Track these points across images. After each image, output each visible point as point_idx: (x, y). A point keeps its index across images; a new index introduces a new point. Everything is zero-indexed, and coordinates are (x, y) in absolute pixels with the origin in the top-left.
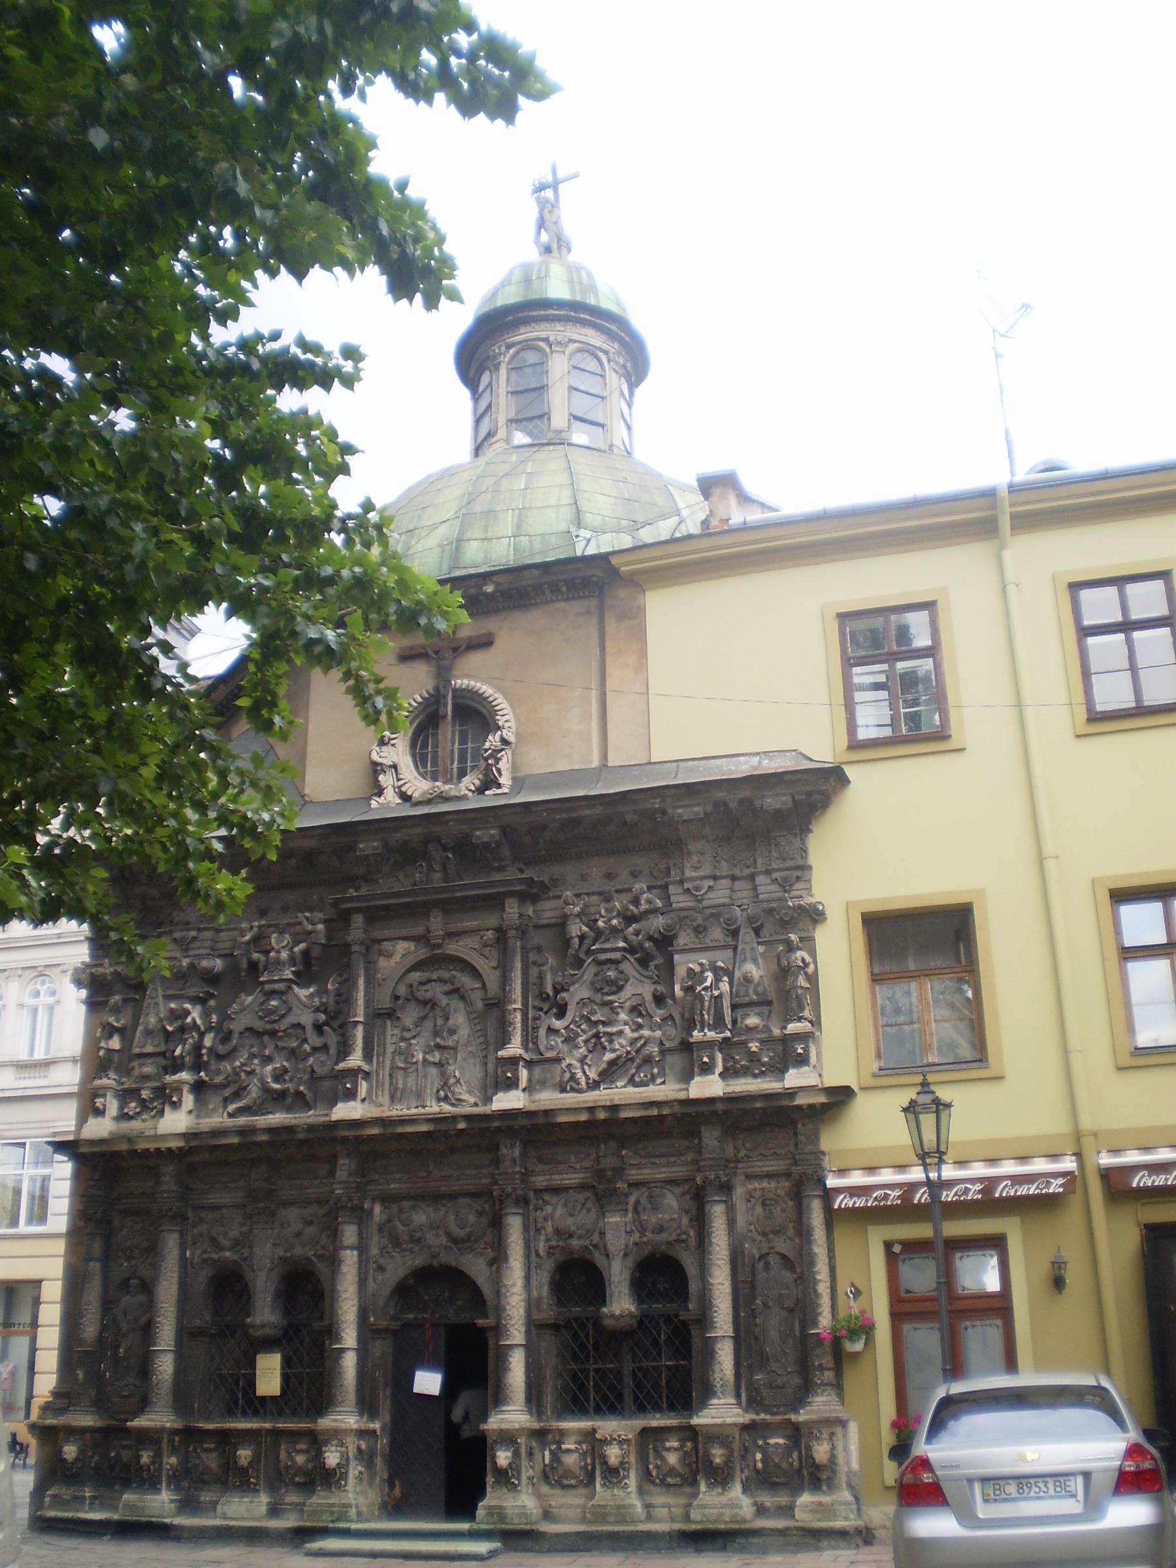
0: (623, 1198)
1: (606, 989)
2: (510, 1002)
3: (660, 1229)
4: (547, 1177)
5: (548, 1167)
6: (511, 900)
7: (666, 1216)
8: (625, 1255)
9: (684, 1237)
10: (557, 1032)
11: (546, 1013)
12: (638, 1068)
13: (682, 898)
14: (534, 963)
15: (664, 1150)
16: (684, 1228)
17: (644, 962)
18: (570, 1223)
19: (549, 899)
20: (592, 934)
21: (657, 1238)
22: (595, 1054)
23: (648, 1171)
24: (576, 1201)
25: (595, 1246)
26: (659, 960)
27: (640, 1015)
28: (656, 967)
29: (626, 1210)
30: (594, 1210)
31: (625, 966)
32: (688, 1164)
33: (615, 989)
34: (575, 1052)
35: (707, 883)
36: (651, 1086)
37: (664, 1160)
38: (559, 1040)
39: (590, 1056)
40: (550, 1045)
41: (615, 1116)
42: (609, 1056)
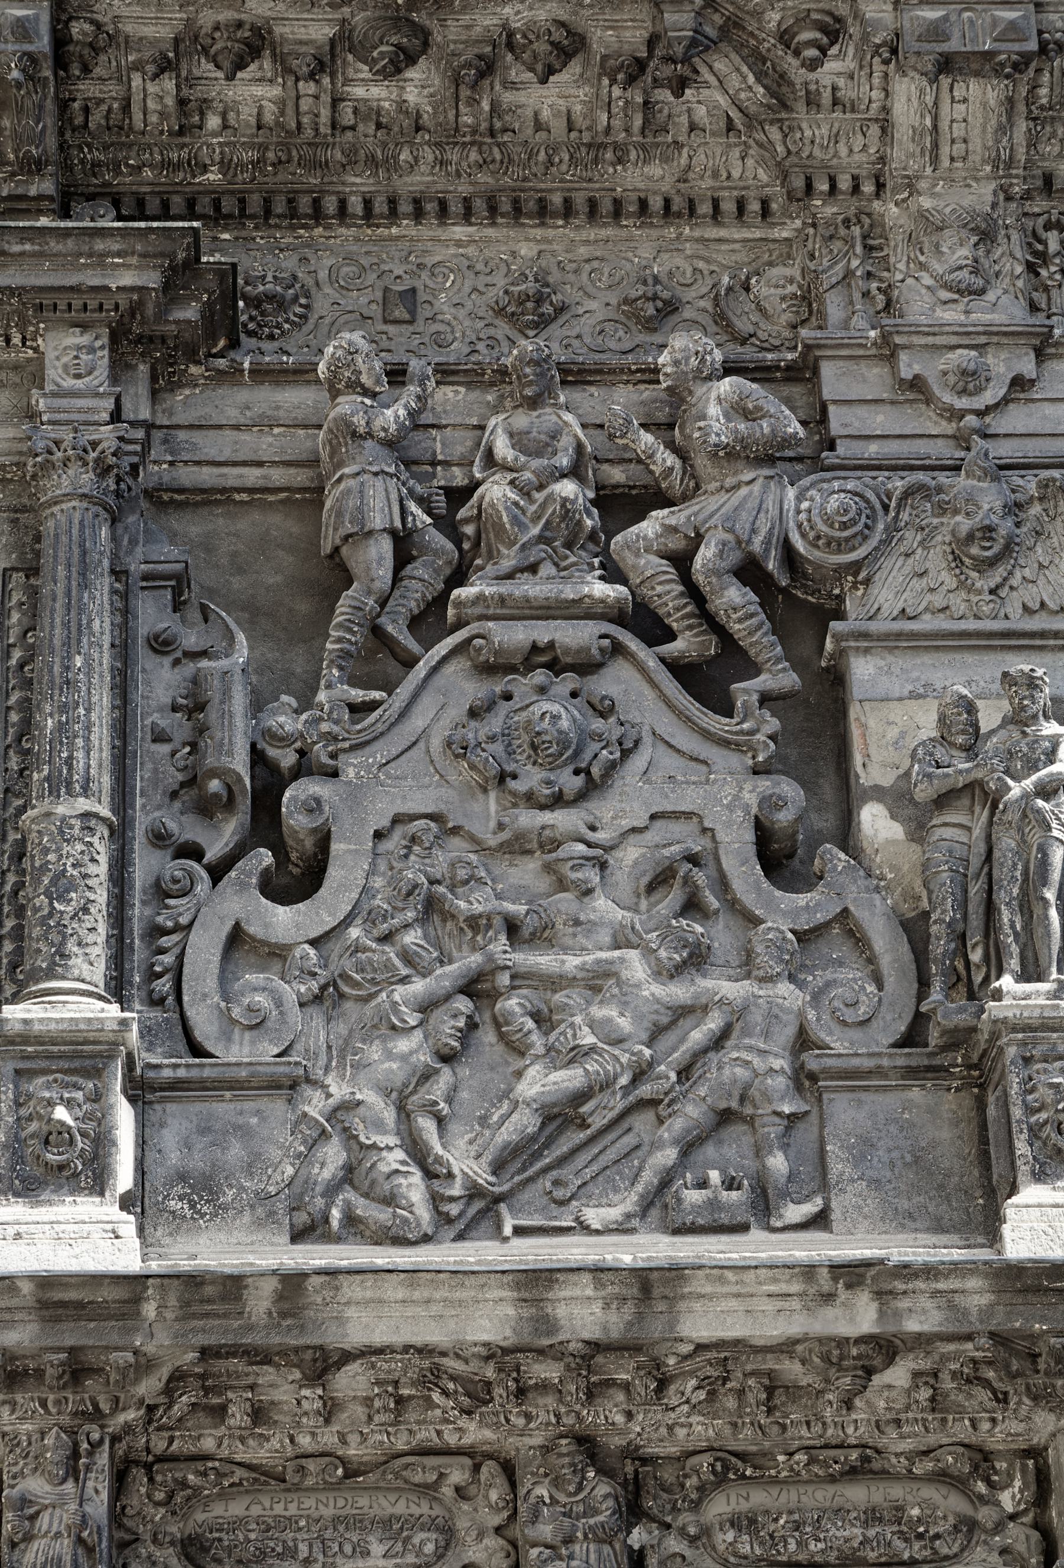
1: (532, 778)
2: (60, 785)
6: (75, 338)
10: (276, 954)
11: (217, 872)
12: (689, 1147)
13: (880, 420)
14: (160, 645)
17: (707, 681)
19: (232, 376)
20: (438, 539)
22: (464, 1072)
26: (779, 677)
27: (692, 906)
28: (766, 699)
31: (616, 682)
33: (572, 783)
34: (374, 1052)
35: (1003, 365)
36: (756, 1234)
38: (290, 993)
39: (446, 1077)
40: (248, 1017)
41: (655, 1329)
42: (541, 1082)
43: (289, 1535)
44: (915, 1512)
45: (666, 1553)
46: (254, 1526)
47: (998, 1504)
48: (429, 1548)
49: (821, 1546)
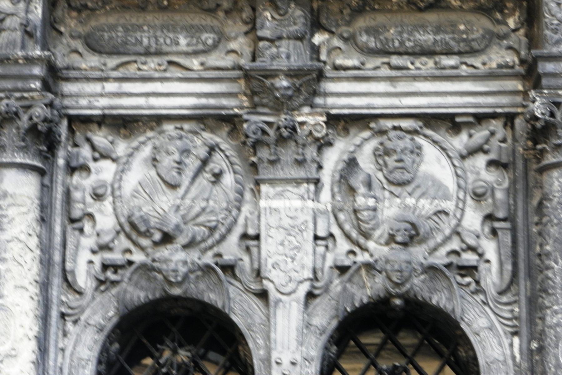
0: (311, 152)
3: (412, 235)
4: (111, 87)
5: (112, 62)
7: (426, 206)
8: (310, 296)
9: (469, 258)
15: (426, 38)
16: (471, 241)
18: (163, 206)
21: (400, 256)
23: (382, 87)
24: (186, 152)
25: (229, 269)
29: (317, 182)
30: (228, 179)
32: (491, 76)
37: (427, 65)
43: (138, 35)
44: (462, 27)
45: (331, 46)
46: (120, 29)
47: (506, 24)
48: (210, 42)
49: (411, 44)
